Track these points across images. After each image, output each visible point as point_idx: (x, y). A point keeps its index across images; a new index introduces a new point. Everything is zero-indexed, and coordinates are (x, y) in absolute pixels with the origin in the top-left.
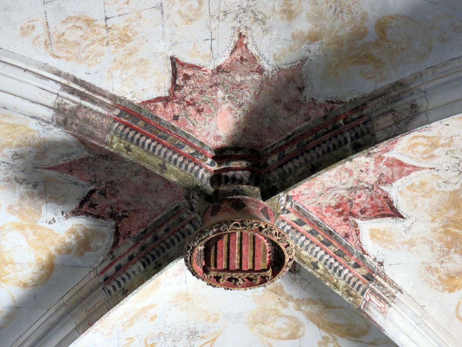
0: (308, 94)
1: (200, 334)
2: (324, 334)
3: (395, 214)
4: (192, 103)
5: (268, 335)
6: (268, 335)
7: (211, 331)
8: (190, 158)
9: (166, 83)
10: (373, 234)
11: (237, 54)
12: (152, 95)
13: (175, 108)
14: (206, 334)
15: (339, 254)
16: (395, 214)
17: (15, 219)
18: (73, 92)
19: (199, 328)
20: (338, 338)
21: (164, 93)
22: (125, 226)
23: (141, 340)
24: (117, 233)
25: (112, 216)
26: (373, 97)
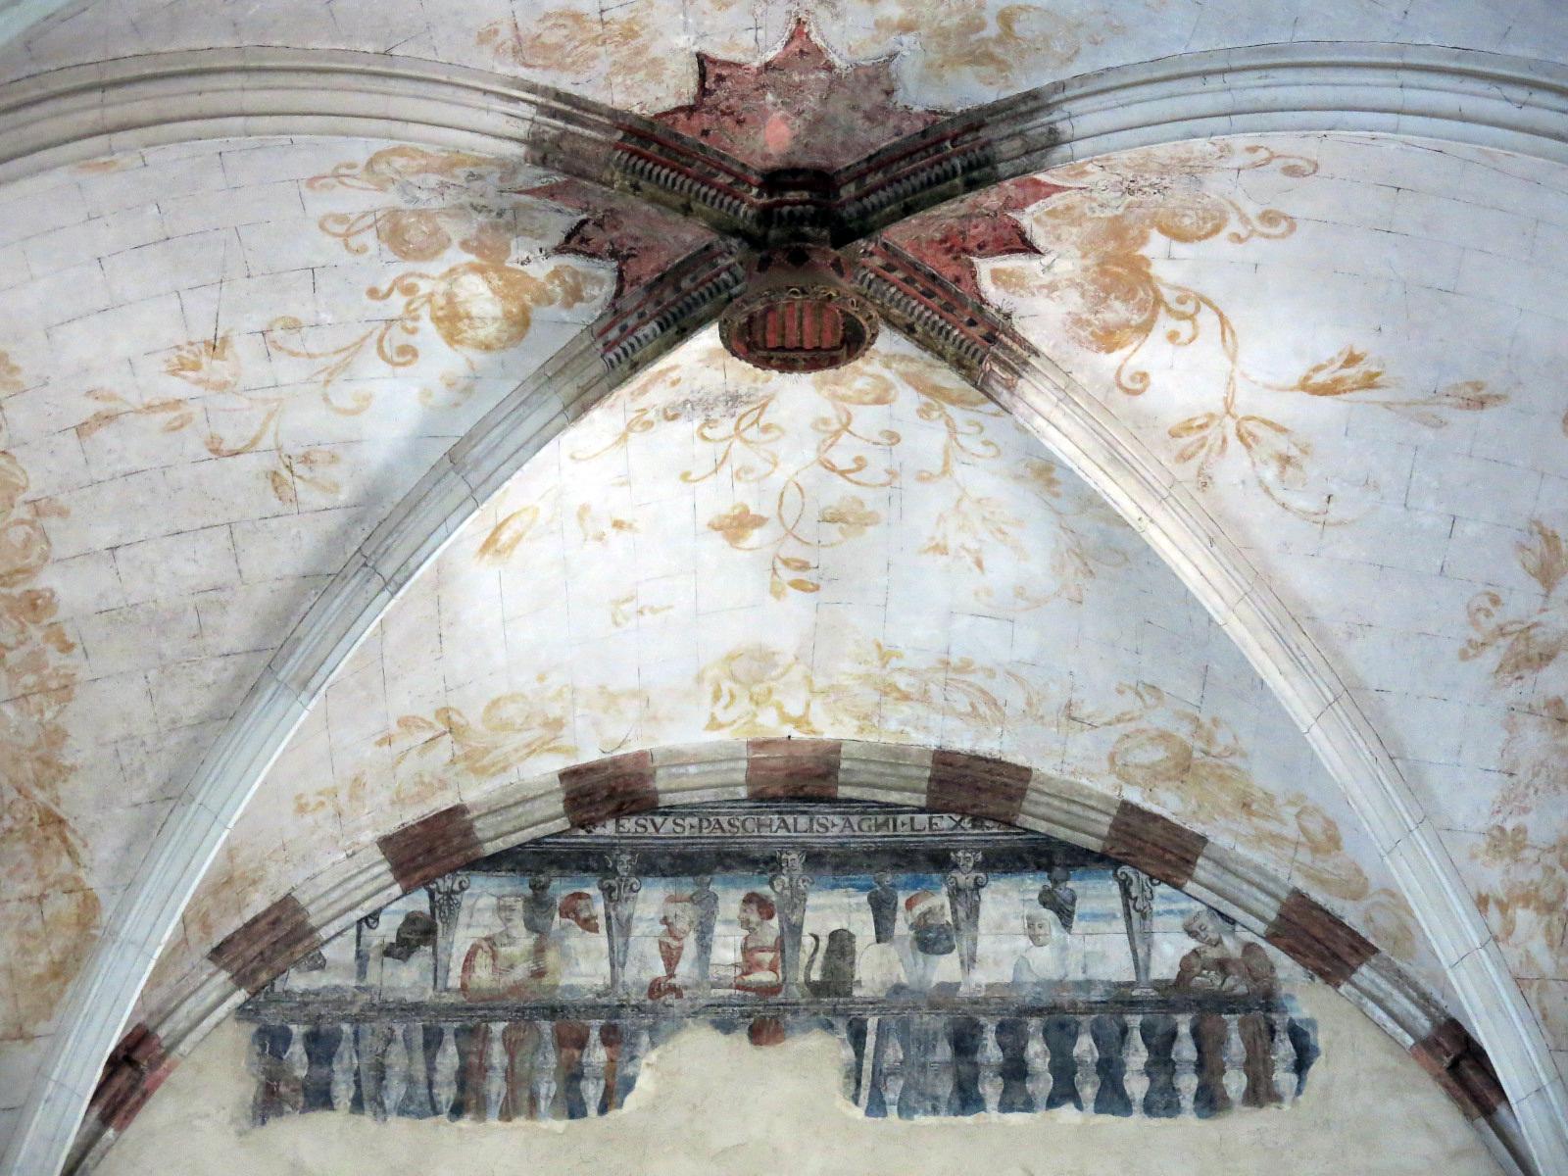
0: (900, 98)
1: (745, 399)
2: (924, 398)
3: (1028, 247)
4: (729, 112)
5: (844, 398)
6: (844, 398)
7: (761, 394)
8: (727, 190)
9: (691, 86)
10: (996, 276)
11: (795, 46)
12: (670, 103)
13: (704, 120)
14: (753, 398)
15: (948, 308)
16: (1028, 247)
17: (472, 258)
18: (554, 114)
19: (743, 390)
20: (946, 405)
21: (687, 100)
22: (633, 268)
23: (657, 411)
24: (621, 279)
25: (614, 254)
26: (995, 110)
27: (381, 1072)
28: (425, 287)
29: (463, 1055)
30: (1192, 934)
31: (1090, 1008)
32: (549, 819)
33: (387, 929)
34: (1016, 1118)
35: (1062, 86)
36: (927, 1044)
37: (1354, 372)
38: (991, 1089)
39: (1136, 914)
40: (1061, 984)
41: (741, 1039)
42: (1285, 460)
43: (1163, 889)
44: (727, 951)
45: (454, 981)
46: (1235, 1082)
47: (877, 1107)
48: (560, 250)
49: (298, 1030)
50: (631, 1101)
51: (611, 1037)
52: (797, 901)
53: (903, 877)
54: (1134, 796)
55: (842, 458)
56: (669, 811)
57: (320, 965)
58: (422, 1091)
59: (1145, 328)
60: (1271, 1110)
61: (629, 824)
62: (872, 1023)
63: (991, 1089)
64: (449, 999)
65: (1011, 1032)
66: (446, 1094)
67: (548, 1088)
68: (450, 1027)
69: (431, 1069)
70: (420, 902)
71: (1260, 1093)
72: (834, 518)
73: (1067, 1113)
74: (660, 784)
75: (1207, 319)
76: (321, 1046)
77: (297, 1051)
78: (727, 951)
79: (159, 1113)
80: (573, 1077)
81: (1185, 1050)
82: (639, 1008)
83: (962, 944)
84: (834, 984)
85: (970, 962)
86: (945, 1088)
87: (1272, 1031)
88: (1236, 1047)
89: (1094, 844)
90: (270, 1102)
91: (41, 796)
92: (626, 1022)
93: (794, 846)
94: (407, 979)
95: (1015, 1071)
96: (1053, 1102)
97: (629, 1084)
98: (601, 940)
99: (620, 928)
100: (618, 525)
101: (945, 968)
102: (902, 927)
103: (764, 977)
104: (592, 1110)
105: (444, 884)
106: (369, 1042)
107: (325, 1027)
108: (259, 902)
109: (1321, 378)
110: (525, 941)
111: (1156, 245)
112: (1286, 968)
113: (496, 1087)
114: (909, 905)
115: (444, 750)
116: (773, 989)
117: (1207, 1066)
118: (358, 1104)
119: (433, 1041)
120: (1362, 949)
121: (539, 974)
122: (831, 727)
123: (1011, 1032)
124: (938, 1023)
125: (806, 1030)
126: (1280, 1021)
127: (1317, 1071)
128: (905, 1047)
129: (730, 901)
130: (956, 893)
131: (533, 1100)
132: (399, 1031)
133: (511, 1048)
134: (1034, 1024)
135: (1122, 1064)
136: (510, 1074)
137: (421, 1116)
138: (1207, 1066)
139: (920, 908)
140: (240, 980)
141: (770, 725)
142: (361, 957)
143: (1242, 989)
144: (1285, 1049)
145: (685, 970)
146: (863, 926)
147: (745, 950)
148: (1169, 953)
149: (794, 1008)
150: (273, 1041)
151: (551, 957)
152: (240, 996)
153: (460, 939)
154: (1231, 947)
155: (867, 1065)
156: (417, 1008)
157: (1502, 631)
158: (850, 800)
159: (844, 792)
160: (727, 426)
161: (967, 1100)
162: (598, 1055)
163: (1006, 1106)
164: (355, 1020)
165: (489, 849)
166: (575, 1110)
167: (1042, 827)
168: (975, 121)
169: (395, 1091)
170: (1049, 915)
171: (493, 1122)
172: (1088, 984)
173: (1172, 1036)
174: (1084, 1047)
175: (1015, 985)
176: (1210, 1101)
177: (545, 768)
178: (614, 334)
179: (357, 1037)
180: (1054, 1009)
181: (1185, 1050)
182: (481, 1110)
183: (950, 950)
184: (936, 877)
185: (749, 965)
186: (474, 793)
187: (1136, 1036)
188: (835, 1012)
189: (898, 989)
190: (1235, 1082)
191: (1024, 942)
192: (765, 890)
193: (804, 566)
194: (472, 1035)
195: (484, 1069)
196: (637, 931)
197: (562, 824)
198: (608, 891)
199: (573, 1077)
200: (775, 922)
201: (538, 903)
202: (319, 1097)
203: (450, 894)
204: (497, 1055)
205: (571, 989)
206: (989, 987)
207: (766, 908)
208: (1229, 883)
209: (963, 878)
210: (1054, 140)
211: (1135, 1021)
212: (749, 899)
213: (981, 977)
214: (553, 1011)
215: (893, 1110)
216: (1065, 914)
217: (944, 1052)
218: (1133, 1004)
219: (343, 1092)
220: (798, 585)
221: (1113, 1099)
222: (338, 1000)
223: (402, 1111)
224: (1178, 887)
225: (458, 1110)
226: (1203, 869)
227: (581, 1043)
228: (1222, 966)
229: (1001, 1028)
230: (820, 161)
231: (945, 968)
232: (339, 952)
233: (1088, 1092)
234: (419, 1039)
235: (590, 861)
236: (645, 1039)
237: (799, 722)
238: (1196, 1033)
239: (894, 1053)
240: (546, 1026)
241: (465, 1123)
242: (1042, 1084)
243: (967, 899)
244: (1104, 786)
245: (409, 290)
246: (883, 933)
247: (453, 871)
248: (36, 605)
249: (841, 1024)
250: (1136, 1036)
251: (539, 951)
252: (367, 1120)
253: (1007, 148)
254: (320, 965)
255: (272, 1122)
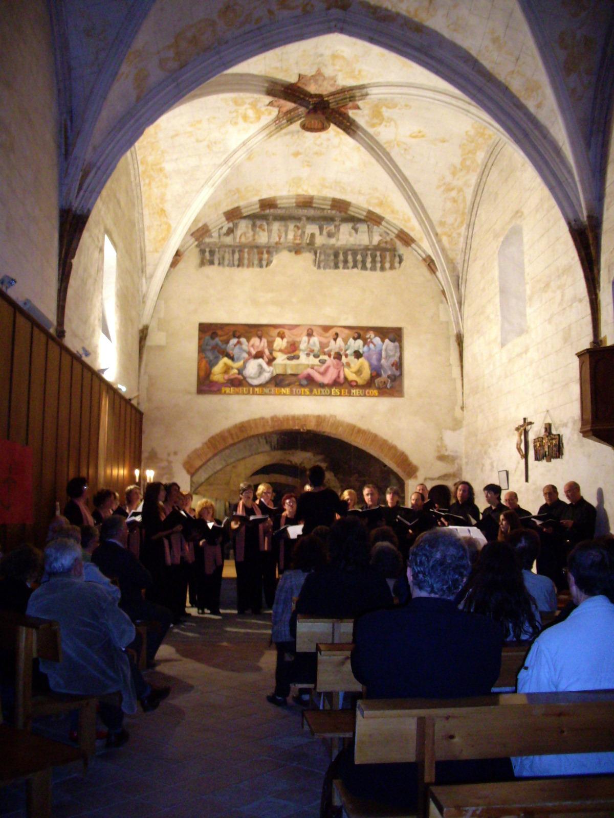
0: (337, 83)
11: (318, 72)
22: (282, 109)
25: (278, 106)
27: (223, 258)
28: (240, 111)
29: (239, 255)
30: (381, 236)
31: (360, 250)
32: (256, 209)
33: (225, 230)
34: (346, 271)
35: (369, 84)
36: (329, 255)
37: (420, 135)
38: (341, 265)
39: (370, 231)
40: (355, 245)
41: (293, 253)
42: (405, 150)
43: (375, 227)
44: (291, 236)
45: (238, 240)
46: (387, 265)
47: (319, 267)
48: (268, 105)
49: (207, 250)
50: (272, 265)
51: (268, 252)
52: (304, 227)
53: (325, 223)
54: (371, 208)
55: (318, 142)
56: (280, 208)
57: (211, 236)
58: (231, 262)
59: (380, 124)
60: (394, 271)
61: (272, 211)
62: (318, 251)
63: (341, 265)
64: (236, 244)
65: (345, 254)
66: (236, 263)
67: (256, 262)
68: (237, 250)
69: (233, 257)
70: (231, 225)
71: (392, 267)
72: (316, 153)
73: (355, 270)
74: (278, 202)
75: (392, 123)
76: (212, 253)
77: (207, 254)
78: (291, 236)
79: (181, 265)
80: (261, 260)
81: (378, 259)
82: (273, 247)
83: (336, 236)
84: (311, 243)
85: (338, 240)
86: (332, 264)
87: (395, 256)
88: (388, 259)
89: (363, 217)
90: (202, 264)
91: (161, 206)
92: (271, 249)
93: (303, 216)
94: (228, 240)
95: (346, 262)
96: (353, 268)
97: (271, 262)
98: (266, 234)
99: (270, 231)
100: (274, 154)
101: (333, 241)
102: (325, 232)
103: (298, 241)
104: (264, 266)
105: (236, 221)
106: (222, 253)
107: (212, 249)
108: (200, 225)
109: (414, 135)
110: (251, 233)
111: (384, 109)
112: (399, 244)
113: (246, 262)
114: (326, 228)
115: (237, 196)
116: (300, 244)
117: (382, 262)
118: (219, 264)
119: (233, 252)
120: (413, 241)
121: (254, 240)
122: (312, 192)
123: (345, 254)
124: (331, 252)
125: (306, 252)
126: (396, 253)
127: (403, 264)
128: (325, 256)
129: (291, 226)
130: (335, 226)
131: (253, 264)
132: (227, 250)
133: (249, 254)
134: (350, 253)
135: (366, 261)
136: (249, 259)
137: (231, 267)
138: (382, 262)
139: (328, 229)
140: (196, 240)
141: (301, 192)
142: (219, 235)
143: (389, 247)
144: (397, 259)
145: (282, 240)
146: (317, 232)
147: (294, 236)
148: (376, 239)
149: (303, 248)
150: (203, 252)
151: (256, 237)
152: (196, 243)
153: (239, 232)
154: (388, 239)
155: (317, 259)
156: (230, 246)
157: (444, 184)
158: (315, 208)
159: (314, 205)
160: (296, 136)
161: (336, 267)
162: (265, 256)
163: (344, 268)
164: (219, 248)
165: (245, 214)
166: (261, 266)
167: (353, 214)
168: (351, 89)
169: (226, 262)
170: (353, 231)
171: (245, 268)
172: (359, 245)
173: (376, 256)
174: (359, 257)
175: (346, 245)
176: (383, 269)
177: (256, 199)
178: (277, 122)
179: (219, 251)
180: (354, 250)
181: (378, 259)
182: (243, 265)
183: (334, 237)
184: (331, 223)
185: (295, 239)
186: (242, 203)
187: (369, 256)
188: (311, 249)
189: (323, 245)
190: (387, 265)
191: (348, 236)
192: (298, 224)
193: (309, 162)
194: (241, 251)
195: (244, 258)
196: (273, 232)
197: (258, 210)
198: (268, 224)
199: (261, 260)
200: (300, 231)
201: (254, 226)
202: (212, 263)
203: (236, 224)
204: (246, 255)
205: (261, 243)
206: (341, 245)
207: (298, 228)
208: (389, 226)
209: (337, 223)
210: (367, 94)
211: (369, 252)
212: (295, 226)
213: (339, 244)
214: (257, 247)
215: (322, 268)
216: (356, 230)
217: (332, 257)
218: (369, 249)
219: (216, 262)
220: (308, 165)
221: (364, 267)
222: (215, 244)
223: (228, 266)
224: (378, 226)
225: (238, 266)
226: (383, 223)
227: (262, 253)
228: (386, 243)
229: (343, 253)
230: (320, 93)
231: (333, 241)
232: (215, 234)
233: (360, 266)
234: (231, 252)
235: (264, 218)
236: (274, 253)
237: (306, 191)
238: (380, 255)
239: (323, 257)
240: (255, 250)
241: (240, 268)
242: (351, 264)
243: (337, 227)
244: (365, 206)
245: (237, 112)
246: (321, 233)
247: (238, 219)
248: (161, 170)
249: (313, 252)
250: (369, 256)
251: (254, 235)
252: (221, 268)
253: (358, 94)
254: (211, 236)
255: (203, 268)
